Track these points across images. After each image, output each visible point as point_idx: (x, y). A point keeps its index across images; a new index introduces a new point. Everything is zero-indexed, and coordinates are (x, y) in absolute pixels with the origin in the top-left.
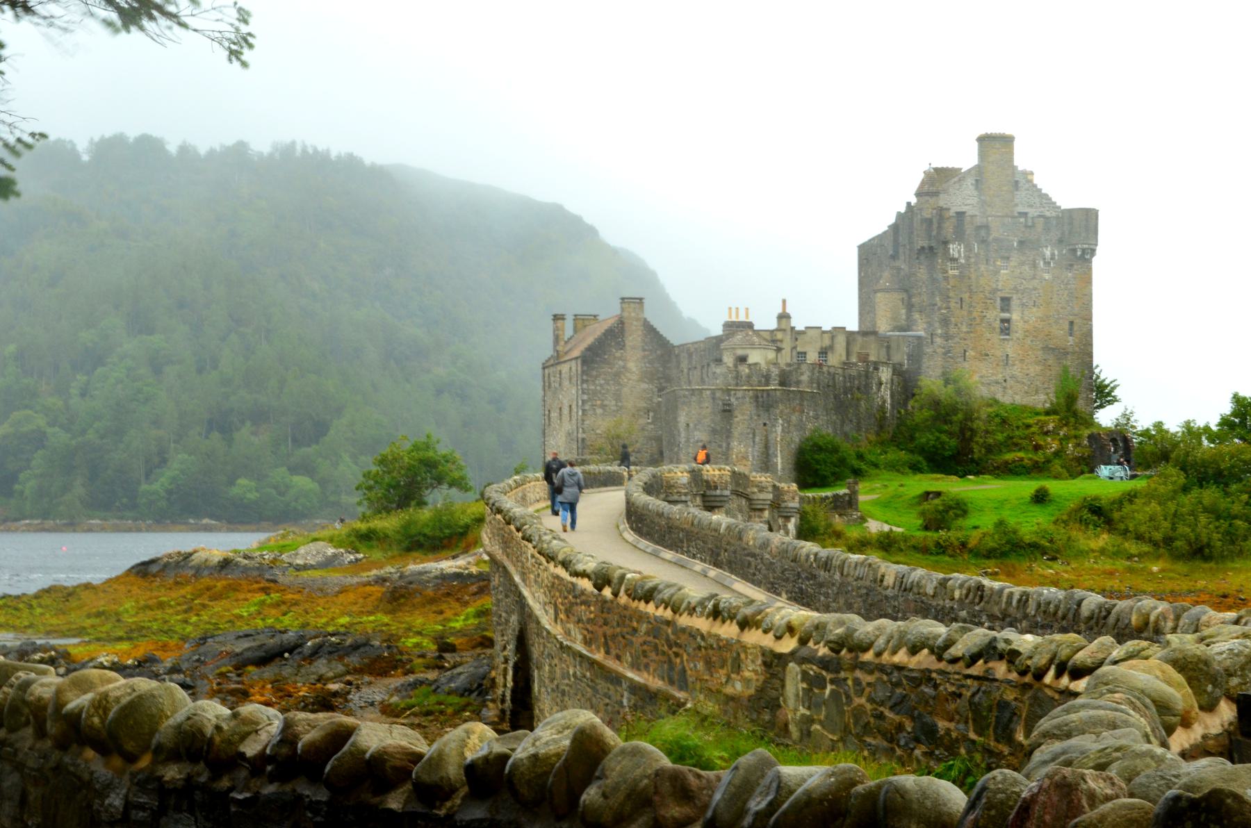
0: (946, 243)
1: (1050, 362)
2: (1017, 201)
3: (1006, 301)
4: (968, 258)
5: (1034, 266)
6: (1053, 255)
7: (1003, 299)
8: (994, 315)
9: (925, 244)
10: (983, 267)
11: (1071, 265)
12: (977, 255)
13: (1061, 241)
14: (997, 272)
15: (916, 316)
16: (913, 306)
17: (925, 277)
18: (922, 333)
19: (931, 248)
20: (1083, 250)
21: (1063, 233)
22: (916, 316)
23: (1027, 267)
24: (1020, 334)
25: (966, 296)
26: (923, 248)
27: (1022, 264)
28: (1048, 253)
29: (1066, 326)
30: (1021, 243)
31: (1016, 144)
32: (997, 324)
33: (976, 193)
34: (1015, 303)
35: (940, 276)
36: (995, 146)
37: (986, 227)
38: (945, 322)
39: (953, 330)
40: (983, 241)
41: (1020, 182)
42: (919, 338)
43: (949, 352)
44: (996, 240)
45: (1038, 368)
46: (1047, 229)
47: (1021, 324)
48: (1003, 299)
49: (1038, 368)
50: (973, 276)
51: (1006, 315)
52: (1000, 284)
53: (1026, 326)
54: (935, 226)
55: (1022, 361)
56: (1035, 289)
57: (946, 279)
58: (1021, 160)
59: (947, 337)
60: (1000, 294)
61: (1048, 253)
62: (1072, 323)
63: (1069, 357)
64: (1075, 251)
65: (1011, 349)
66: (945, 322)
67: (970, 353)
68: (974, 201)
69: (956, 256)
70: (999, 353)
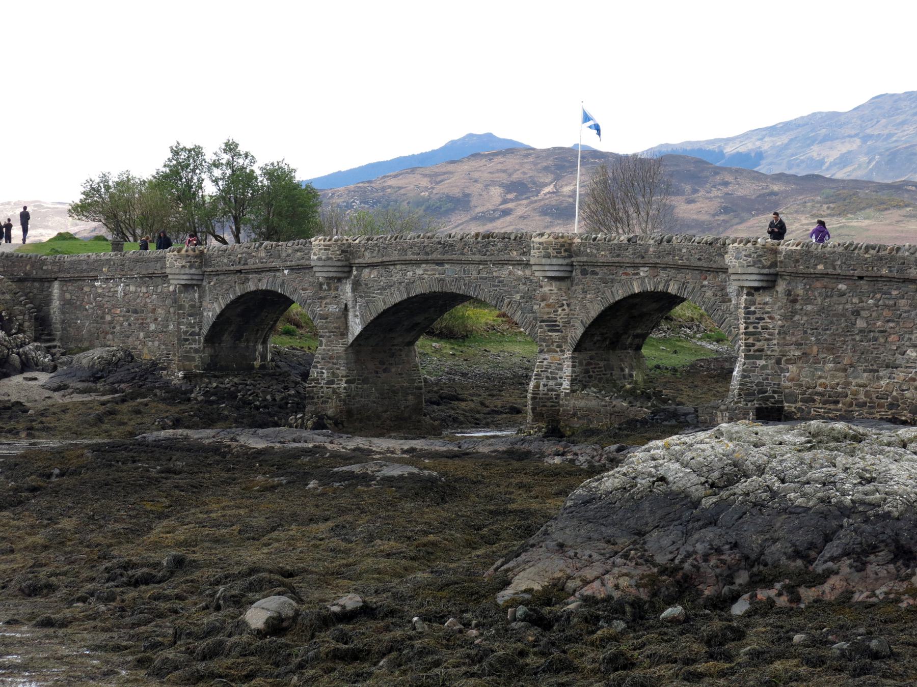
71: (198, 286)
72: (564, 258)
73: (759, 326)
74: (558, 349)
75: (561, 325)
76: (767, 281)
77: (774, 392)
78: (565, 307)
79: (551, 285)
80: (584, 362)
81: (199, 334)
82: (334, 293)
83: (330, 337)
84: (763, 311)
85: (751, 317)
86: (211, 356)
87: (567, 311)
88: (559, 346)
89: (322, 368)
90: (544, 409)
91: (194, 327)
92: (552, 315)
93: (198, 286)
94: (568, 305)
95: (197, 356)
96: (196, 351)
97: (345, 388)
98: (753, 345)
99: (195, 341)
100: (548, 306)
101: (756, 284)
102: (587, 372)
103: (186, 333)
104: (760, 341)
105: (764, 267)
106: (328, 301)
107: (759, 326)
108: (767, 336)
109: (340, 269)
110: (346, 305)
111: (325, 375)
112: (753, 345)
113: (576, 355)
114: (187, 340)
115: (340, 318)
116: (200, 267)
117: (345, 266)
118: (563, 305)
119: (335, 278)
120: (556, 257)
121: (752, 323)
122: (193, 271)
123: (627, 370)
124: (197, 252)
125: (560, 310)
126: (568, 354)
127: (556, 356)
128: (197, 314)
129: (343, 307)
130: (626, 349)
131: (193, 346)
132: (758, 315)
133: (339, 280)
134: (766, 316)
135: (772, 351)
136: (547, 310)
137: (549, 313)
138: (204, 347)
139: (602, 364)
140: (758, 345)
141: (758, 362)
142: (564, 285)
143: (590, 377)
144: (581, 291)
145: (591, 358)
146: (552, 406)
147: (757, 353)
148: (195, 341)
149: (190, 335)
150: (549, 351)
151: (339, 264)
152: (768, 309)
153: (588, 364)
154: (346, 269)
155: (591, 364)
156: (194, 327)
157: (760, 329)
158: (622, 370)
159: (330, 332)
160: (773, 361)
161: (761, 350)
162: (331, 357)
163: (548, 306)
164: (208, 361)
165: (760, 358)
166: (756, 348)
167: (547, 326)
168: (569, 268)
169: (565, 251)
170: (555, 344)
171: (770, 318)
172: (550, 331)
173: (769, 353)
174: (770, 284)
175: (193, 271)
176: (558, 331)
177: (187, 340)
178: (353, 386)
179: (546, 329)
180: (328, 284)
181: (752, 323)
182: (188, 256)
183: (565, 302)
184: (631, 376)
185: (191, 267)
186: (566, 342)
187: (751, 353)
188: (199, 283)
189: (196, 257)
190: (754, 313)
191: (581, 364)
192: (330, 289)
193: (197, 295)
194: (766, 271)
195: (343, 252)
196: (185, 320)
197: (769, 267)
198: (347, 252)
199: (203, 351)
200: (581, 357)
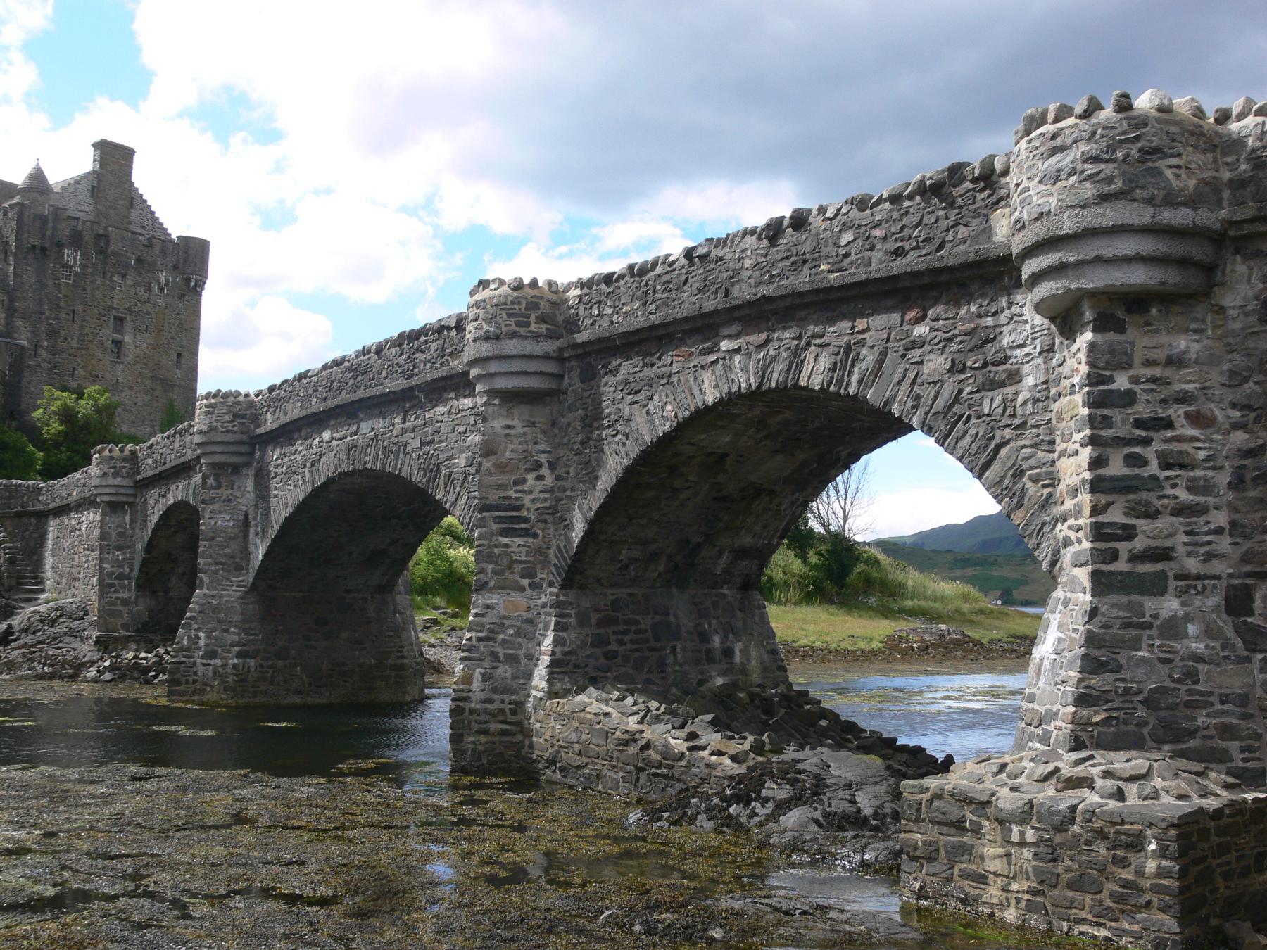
0: (60, 246)
1: (157, 393)
2: (131, 219)
3: (120, 320)
4: (83, 267)
5: (149, 289)
6: (167, 280)
7: (116, 318)
8: (107, 334)
9: (38, 243)
10: (99, 280)
11: (183, 295)
12: (95, 265)
13: (175, 267)
14: (112, 289)
15: (19, 323)
16: (16, 310)
17: (33, 280)
18: (25, 343)
19: (43, 249)
20: (197, 281)
21: (178, 261)
22: (19, 323)
23: (142, 289)
24: (130, 359)
25: (79, 308)
26: (34, 247)
27: (137, 284)
28: (163, 279)
29: (174, 358)
30: (139, 260)
31: (136, 158)
32: (109, 345)
33: (91, 201)
34: (128, 324)
35: (50, 283)
36: (115, 159)
37: (106, 237)
38: (53, 333)
39: (61, 344)
40: (102, 251)
41: (133, 200)
42: (22, 347)
43: (55, 367)
44: (115, 253)
45: (147, 398)
46: (164, 253)
47: (132, 348)
48: (116, 318)
49: (147, 398)
50: (89, 287)
51: (118, 337)
52: (115, 301)
53: (137, 351)
54: (50, 225)
55: (131, 388)
56: (148, 313)
57: (58, 286)
58: (144, 178)
59: (54, 351)
60: (113, 312)
61: (163, 279)
62: (179, 355)
63: (176, 390)
64: (188, 281)
65: (121, 373)
66: (53, 333)
67: (80, 372)
68: (90, 208)
69: (71, 262)
70: (108, 376)
71: (131, 505)
72: (536, 337)
73: (1150, 453)
74: (525, 582)
75: (533, 516)
76: (1183, 263)
77: (1227, 732)
78: (545, 471)
79: (510, 415)
80: (594, 619)
81: (128, 577)
82: (225, 493)
83: (216, 572)
84: (1165, 392)
85: (1117, 415)
86: (150, 611)
87: (549, 480)
88: (528, 573)
89: (199, 629)
90: (483, 738)
91: (122, 567)
92: (511, 493)
93: (131, 505)
94: (552, 466)
95: (125, 610)
96: (125, 602)
97: (234, 666)
98: (1128, 533)
99: (123, 587)
100: (502, 468)
101: (1137, 277)
102: (599, 642)
103: (110, 574)
104: (1152, 515)
105: (1170, 200)
106: (215, 507)
107: (1150, 453)
108: (1183, 495)
109: (231, 449)
110: (246, 515)
111: (202, 643)
112: (1128, 533)
113: (570, 596)
114: (112, 585)
115: (235, 538)
116: (129, 475)
117: (242, 443)
118: (538, 466)
119: (228, 465)
120: (513, 335)
121: (1120, 442)
122: (118, 481)
123: (717, 640)
124: (127, 453)
125: (531, 478)
126: (550, 594)
127: (520, 599)
128: (128, 547)
129: (242, 518)
130: (715, 586)
131: (120, 595)
132: (1142, 410)
133: (236, 469)
134: (1177, 412)
135: (1210, 557)
136: (499, 478)
137: (501, 487)
138: (137, 597)
139: (646, 622)
140: (1147, 533)
141: (1150, 604)
142: (542, 415)
143: (610, 656)
144: (578, 424)
145: (616, 605)
146: (504, 733)
147: (1146, 568)
148: (123, 587)
149: (117, 578)
150: (499, 587)
151: (229, 438)
152: (1184, 382)
153: (607, 621)
154: (244, 449)
155: (615, 621)
156: (122, 567)
157: (1153, 468)
158: (704, 638)
159: (217, 563)
160: (1212, 601)
161: (1165, 555)
162: (216, 610)
163: (502, 468)
164: (145, 618)
165: (1157, 586)
166: (1139, 543)
167: (498, 520)
168: (550, 367)
169: (542, 319)
170: (518, 568)
171: (1196, 419)
172: (505, 533)
173: (1193, 565)
174: (1194, 280)
175: (118, 481)
176: (525, 533)
177: (112, 585)
178: (252, 662)
179: (495, 527)
180: (217, 478)
181: (1120, 442)
182: (112, 458)
183: (543, 458)
184: (728, 653)
185: (115, 475)
186: (545, 563)
187: (1122, 565)
188: (131, 499)
189: (124, 460)
190: (1128, 398)
191: (583, 620)
192: (218, 487)
193: (128, 518)
194: (1179, 216)
195: (236, 416)
196: (110, 556)
197: (1192, 203)
198: (244, 417)
199: (136, 603)
200: (586, 603)
